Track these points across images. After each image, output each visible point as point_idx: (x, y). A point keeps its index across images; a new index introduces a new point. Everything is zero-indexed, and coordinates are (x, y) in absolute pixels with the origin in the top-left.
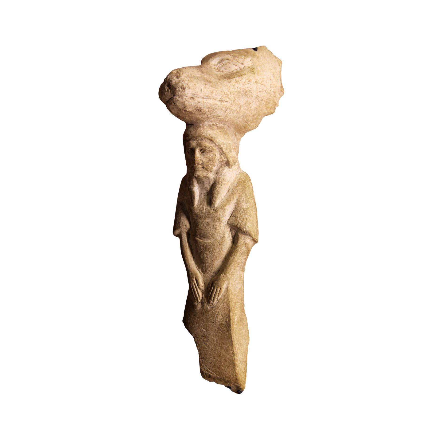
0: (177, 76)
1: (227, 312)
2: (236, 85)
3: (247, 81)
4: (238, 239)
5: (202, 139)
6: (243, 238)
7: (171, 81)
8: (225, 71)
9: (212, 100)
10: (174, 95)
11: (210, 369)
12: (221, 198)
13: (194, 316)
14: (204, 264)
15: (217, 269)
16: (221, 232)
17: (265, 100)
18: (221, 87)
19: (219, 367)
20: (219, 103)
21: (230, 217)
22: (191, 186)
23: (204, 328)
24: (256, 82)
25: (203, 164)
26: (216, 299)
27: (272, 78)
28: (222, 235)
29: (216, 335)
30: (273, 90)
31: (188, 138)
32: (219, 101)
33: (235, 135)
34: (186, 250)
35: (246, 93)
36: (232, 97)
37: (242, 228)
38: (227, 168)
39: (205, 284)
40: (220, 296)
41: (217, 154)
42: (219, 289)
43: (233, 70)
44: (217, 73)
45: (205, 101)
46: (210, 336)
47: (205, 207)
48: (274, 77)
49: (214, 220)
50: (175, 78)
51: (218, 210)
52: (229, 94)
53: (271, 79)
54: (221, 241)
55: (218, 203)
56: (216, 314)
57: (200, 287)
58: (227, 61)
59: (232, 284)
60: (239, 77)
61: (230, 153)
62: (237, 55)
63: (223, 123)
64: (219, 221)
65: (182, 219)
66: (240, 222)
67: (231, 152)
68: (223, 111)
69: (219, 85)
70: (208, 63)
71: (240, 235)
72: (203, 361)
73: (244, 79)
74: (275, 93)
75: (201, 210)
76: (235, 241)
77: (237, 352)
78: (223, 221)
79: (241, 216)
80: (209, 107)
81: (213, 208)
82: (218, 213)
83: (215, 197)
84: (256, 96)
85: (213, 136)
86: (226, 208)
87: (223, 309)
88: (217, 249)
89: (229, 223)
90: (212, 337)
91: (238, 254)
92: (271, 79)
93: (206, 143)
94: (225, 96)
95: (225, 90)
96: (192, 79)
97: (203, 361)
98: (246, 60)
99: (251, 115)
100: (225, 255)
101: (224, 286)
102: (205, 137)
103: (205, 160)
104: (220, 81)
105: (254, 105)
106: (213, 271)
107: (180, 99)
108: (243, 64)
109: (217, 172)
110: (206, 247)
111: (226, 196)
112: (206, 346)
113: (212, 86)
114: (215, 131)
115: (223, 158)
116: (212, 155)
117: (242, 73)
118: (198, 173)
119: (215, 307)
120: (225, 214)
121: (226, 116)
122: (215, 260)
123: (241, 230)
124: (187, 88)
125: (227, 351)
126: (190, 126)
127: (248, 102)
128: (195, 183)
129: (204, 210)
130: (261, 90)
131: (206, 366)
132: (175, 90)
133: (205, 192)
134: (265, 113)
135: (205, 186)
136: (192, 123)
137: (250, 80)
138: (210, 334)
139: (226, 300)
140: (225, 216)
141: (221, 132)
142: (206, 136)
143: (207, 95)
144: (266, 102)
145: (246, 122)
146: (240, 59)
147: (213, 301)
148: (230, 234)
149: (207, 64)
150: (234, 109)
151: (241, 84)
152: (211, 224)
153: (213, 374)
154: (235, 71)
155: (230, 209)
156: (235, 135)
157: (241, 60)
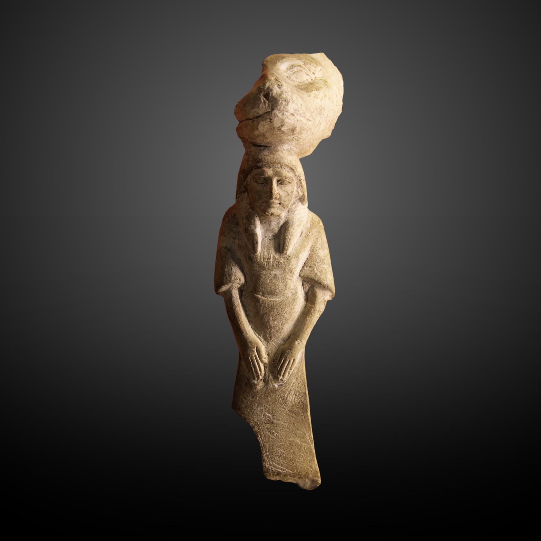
0: (279, 85)
1: (302, 389)
4: (314, 295)
5: (281, 167)
6: (322, 294)
7: (272, 90)
12: (293, 244)
13: (253, 398)
14: (268, 329)
15: (286, 334)
16: (292, 287)
19: (292, 460)
21: (303, 267)
24: (329, 98)
25: (280, 199)
26: (287, 374)
28: (294, 291)
31: (260, 164)
34: (239, 312)
37: (322, 281)
38: (300, 204)
39: (268, 355)
40: (292, 370)
46: (278, 422)
47: (272, 253)
50: (276, 87)
54: (293, 298)
55: (291, 248)
57: (264, 359)
58: (299, 68)
65: (234, 270)
66: (318, 273)
72: (267, 456)
75: (267, 259)
76: (310, 298)
79: (318, 267)
81: (285, 256)
82: (290, 262)
83: (287, 241)
87: (297, 386)
88: (288, 309)
90: (282, 423)
93: (286, 172)
97: (267, 456)
100: (297, 317)
102: (286, 165)
103: (283, 194)
106: (281, 337)
107: (280, 115)
108: (314, 74)
110: (272, 307)
112: (272, 436)
116: (290, 188)
119: (286, 383)
122: (285, 324)
123: (320, 283)
124: (291, 102)
125: (303, 438)
126: (262, 148)
131: (273, 461)
132: (277, 103)
133: (270, 235)
135: (272, 228)
138: (279, 419)
140: (297, 266)
142: (287, 163)
146: (312, 68)
147: (283, 376)
152: (280, 276)
155: (304, 257)
157: (313, 69)
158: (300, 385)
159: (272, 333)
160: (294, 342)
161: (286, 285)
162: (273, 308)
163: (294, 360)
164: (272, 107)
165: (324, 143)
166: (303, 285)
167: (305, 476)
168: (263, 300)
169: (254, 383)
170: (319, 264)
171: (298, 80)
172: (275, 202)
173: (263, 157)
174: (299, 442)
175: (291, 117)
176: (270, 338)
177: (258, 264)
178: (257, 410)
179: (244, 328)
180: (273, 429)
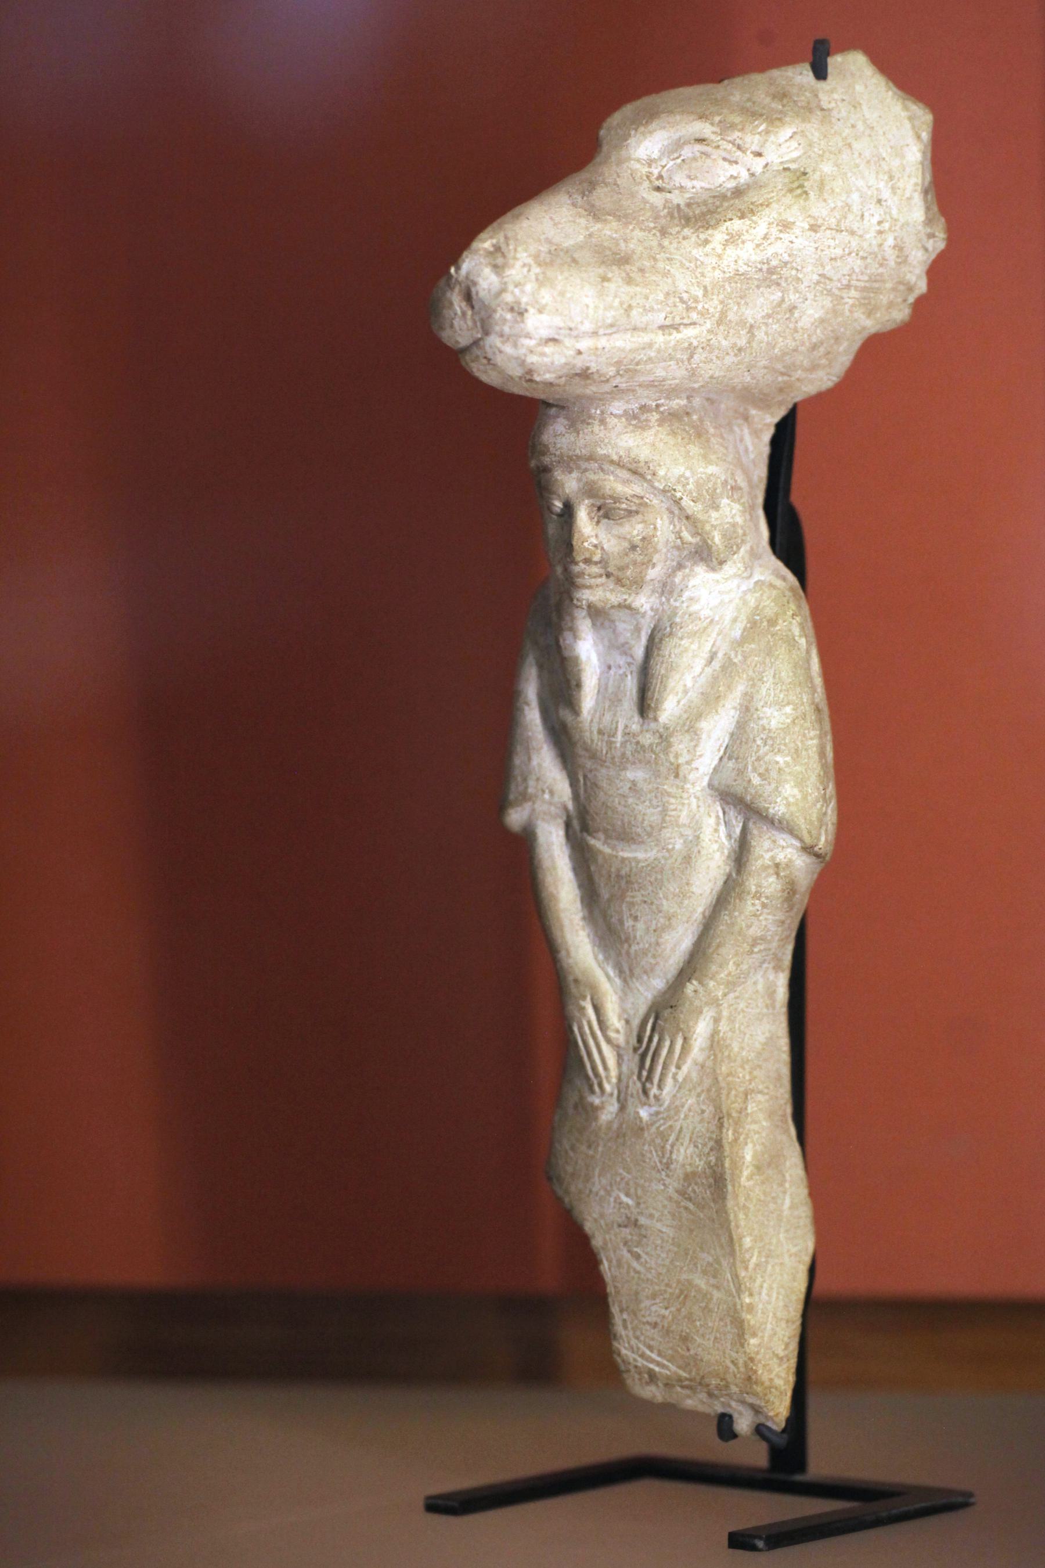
1: (713, 1128)
2: (731, 252)
3: (774, 231)
5: (602, 470)
6: (767, 844)
7: (475, 284)
8: (688, 184)
9: (628, 335)
10: (487, 333)
11: (650, 1348)
13: (589, 1147)
14: (622, 943)
16: (684, 817)
17: (858, 284)
18: (666, 274)
19: (685, 1339)
20: (660, 339)
21: (721, 759)
22: (568, 636)
23: (627, 1195)
25: (603, 562)
26: (669, 1081)
27: (886, 194)
28: (688, 832)
29: (673, 1215)
30: (890, 241)
32: (662, 328)
33: (746, 418)
35: (771, 275)
36: (713, 305)
37: (762, 804)
38: (700, 570)
39: (627, 1022)
40: (685, 1069)
41: (659, 521)
42: (679, 1042)
43: (722, 179)
44: (657, 199)
45: (603, 342)
48: (894, 189)
49: (657, 774)
51: (671, 735)
52: (700, 293)
53: (879, 201)
56: (672, 1138)
57: (612, 1034)
58: (698, 147)
59: (731, 1020)
60: (742, 217)
61: (714, 514)
62: (737, 119)
63: (684, 395)
64: (677, 776)
66: (756, 780)
67: (717, 508)
68: (679, 361)
69: (660, 265)
70: (623, 153)
71: (755, 832)
73: (762, 224)
74: (901, 249)
77: (752, 1279)
78: (691, 777)
79: (758, 759)
80: (619, 363)
82: (669, 745)
84: (815, 277)
85: (644, 453)
86: (704, 725)
87: (697, 1118)
88: (673, 887)
89: (716, 783)
90: (659, 1226)
91: (751, 905)
92: (879, 201)
93: (616, 484)
94: (681, 306)
95: (683, 281)
96: (550, 273)
98: (772, 138)
99: (802, 349)
101: (701, 1029)
102: (612, 462)
104: (666, 243)
105: (811, 311)
107: (508, 349)
108: (759, 155)
109: (664, 585)
111: (703, 680)
112: (635, 1264)
113: (629, 281)
114: (649, 435)
115: (686, 536)
116: (640, 527)
117: (753, 197)
118: (586, 596)
119: (668, 1109)
120: (699, 750)
121: (693, 374)
124: (531, 310)
125: (715, 1277)
127: (784, 306)
128: (584, 625)
130: (839, 252)
131: (637, 1338)
134: (864, 328)
135: (622, 640)
136: (561, 404)
137: (786, 226)
138: (651, 1216)
139: (707, 1082)
140: (704, 757)
141: (673, 433)
142: (615, 458)
143: (609, 321)
144: (864, 289)
145: (782, 374)
147: (660, 1087)
148: (722, 828)
149: (620, 163)
150: (724, 343)
151: (750, 246)
152: (646, 787)
153: (663, 1366)
154: (731, 184)
155: (716, 729)
156: (746, 418)
157: (753, 141)
158: (706, 1115)
161: (664, 812)
164: (482, 327)
165: (875, 350)
167: (717, 1387)
169: (592, 1104)
171: (698, 184)
172: (588, 573)
174: (703, 1286)
175: (548, 349)
176: (631, 970)
177: (586, 750)
178: (599, 1183)
179: (563, 937)
180: (639, 1244)
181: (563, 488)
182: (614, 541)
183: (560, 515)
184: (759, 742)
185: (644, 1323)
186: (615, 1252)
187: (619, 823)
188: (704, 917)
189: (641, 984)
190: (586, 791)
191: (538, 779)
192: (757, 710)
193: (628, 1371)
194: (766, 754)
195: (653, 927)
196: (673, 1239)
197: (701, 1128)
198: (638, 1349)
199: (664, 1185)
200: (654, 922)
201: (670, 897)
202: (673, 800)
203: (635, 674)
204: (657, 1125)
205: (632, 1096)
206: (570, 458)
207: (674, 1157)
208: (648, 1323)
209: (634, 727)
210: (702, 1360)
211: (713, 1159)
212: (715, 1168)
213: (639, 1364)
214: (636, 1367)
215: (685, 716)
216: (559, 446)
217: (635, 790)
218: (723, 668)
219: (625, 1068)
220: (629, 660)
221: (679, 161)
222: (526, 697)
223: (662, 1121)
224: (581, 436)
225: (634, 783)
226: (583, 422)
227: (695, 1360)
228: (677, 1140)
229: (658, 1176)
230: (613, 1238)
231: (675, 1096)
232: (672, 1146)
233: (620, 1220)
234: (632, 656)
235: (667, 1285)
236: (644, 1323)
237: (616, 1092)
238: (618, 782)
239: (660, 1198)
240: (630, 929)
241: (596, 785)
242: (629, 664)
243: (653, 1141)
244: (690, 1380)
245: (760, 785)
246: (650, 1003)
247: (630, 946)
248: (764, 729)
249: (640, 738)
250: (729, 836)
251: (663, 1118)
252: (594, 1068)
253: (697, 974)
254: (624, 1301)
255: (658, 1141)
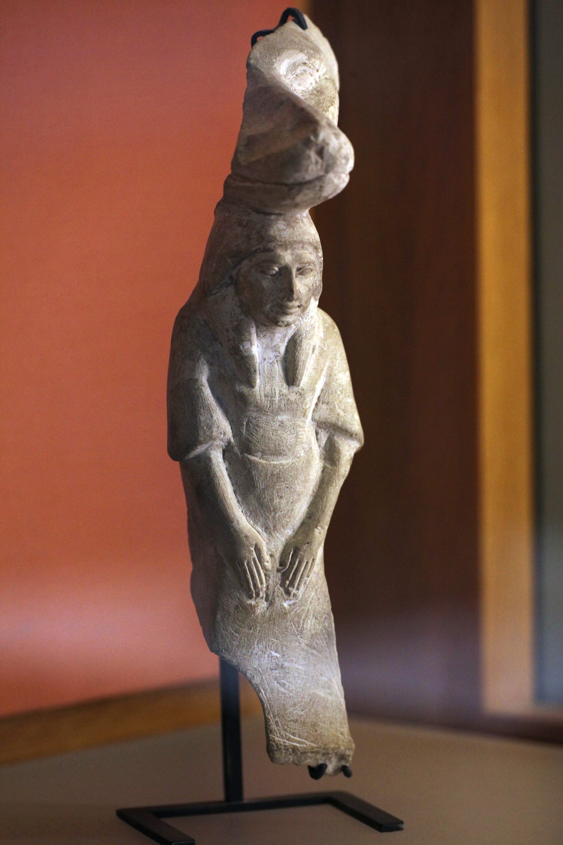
6: (347, 448)
7: (328, 144)
10: (327, 171)
11: (294, 734)
13: (250, 629)
23: (276, 652)
57: (266, 564)
66: (342, 414)
71: (340, 442)
72: (277, 723)
76: (331, 454)
79: (340, 402)
87: (316, 603)
88: (302, 478)
89: (317, 418)
90: (296, 666)
97: (277, 723)
110: (277, 477)
112: (282, 689)
125: (329, 688)
129: (277, 395)
131: (285, 730)
138: (292, 661)
147: (298, 589)
152: (288, 424)
153: (302, 743)
158: (321, 600)
159: (277, 519)
160: (314, 531)
161: (297, 437)
162: (279, 478)
163: (313, 560)
166: (317, 433)
168: (263, 466)
169: (251, 605)
170: (341, 397)
173: (277, 233)
174: (323, 695)
177: (257, 407)
178: (257, 649)
180: (284, 678)
181: (284, 260)
182: (303, 287)
183: (273, 275)
184: (339, 393)
185: (289, 721)
186: (268, 685)
187: (273, 445)
188: (314, 492)
189: (279, 534)
190: (247, 430)
191: (218, 427)
192: (335, 375)
193: (279, 749)
194: (343, 399)
195: (291, 501)
196: (305, 671)
197: (319, 608)
198: (286, 736)
199: (299, 642)
200: (292, 498)
201: (300, 483)
202: (301, 429)
203: (279, 362)
204: (295, 610)
205: (278, 596)
206: (290, 242)
207: (305, 626)
208: (291, 720)
209: (284, 391)
210: (324, 736)
211: (326, 624)
212: (328, 629)
213: (287, 744)
214: (285, 746)
215: (310, 382)
216: (283, 236)
217: (283, 426)
218: (320, 354)
219: (271, 582)
220: (277, 354)
221: (294, 76)
222: (202, 381)
223: (298, 608)
224: (295, 229)
225: (282, 422)
226: (294, 222)
227: (321, 736)
228: (306, 616)
229: (296, 638)
230: (268, 677)
231: (304, 593)
232: (304, 620)
233: (272, 667)
234: (279, 352)
235: (302, 698)
236: (289, 721)
237: (265, 596)
238: (272, 422)
239: (297, 650)
240: (278, 504)
241: (258, 426)
242: (276, 357)
243: (293, 619)
244: (318, 748)
245: (345, 416)
246: (284, 543)
247: (276, 513)
248: (340, 385)
249: (289, 397)
250: (320, 446)
251: (299, 606)
252: (255, 585)
253: (321, 523)
254: (276, 711)
255: (296, 619)
